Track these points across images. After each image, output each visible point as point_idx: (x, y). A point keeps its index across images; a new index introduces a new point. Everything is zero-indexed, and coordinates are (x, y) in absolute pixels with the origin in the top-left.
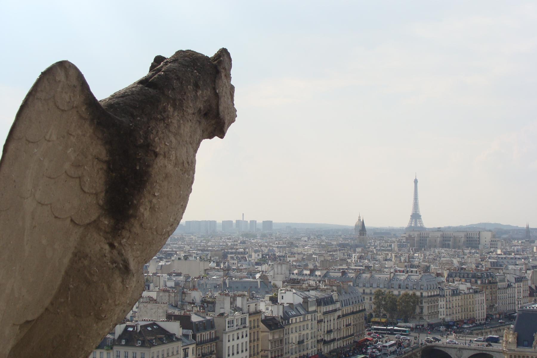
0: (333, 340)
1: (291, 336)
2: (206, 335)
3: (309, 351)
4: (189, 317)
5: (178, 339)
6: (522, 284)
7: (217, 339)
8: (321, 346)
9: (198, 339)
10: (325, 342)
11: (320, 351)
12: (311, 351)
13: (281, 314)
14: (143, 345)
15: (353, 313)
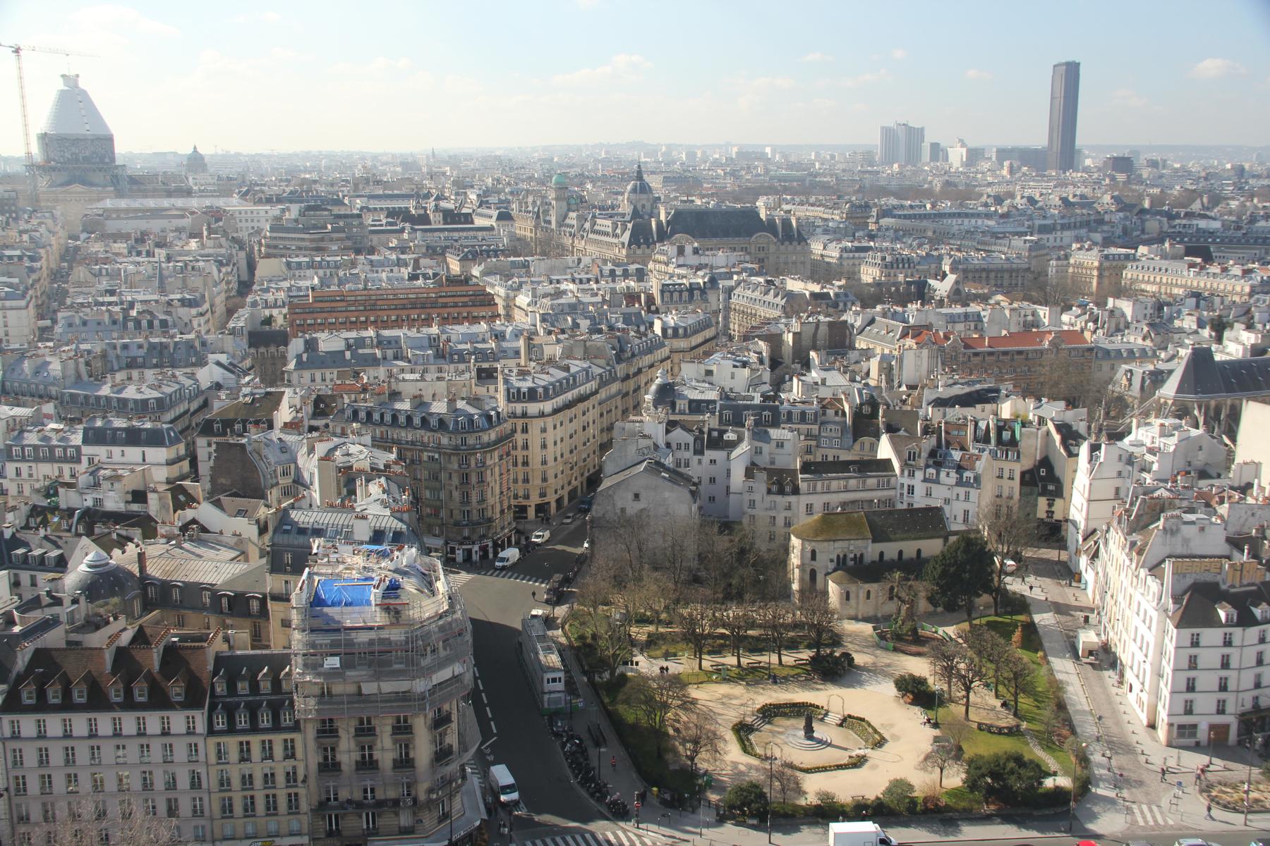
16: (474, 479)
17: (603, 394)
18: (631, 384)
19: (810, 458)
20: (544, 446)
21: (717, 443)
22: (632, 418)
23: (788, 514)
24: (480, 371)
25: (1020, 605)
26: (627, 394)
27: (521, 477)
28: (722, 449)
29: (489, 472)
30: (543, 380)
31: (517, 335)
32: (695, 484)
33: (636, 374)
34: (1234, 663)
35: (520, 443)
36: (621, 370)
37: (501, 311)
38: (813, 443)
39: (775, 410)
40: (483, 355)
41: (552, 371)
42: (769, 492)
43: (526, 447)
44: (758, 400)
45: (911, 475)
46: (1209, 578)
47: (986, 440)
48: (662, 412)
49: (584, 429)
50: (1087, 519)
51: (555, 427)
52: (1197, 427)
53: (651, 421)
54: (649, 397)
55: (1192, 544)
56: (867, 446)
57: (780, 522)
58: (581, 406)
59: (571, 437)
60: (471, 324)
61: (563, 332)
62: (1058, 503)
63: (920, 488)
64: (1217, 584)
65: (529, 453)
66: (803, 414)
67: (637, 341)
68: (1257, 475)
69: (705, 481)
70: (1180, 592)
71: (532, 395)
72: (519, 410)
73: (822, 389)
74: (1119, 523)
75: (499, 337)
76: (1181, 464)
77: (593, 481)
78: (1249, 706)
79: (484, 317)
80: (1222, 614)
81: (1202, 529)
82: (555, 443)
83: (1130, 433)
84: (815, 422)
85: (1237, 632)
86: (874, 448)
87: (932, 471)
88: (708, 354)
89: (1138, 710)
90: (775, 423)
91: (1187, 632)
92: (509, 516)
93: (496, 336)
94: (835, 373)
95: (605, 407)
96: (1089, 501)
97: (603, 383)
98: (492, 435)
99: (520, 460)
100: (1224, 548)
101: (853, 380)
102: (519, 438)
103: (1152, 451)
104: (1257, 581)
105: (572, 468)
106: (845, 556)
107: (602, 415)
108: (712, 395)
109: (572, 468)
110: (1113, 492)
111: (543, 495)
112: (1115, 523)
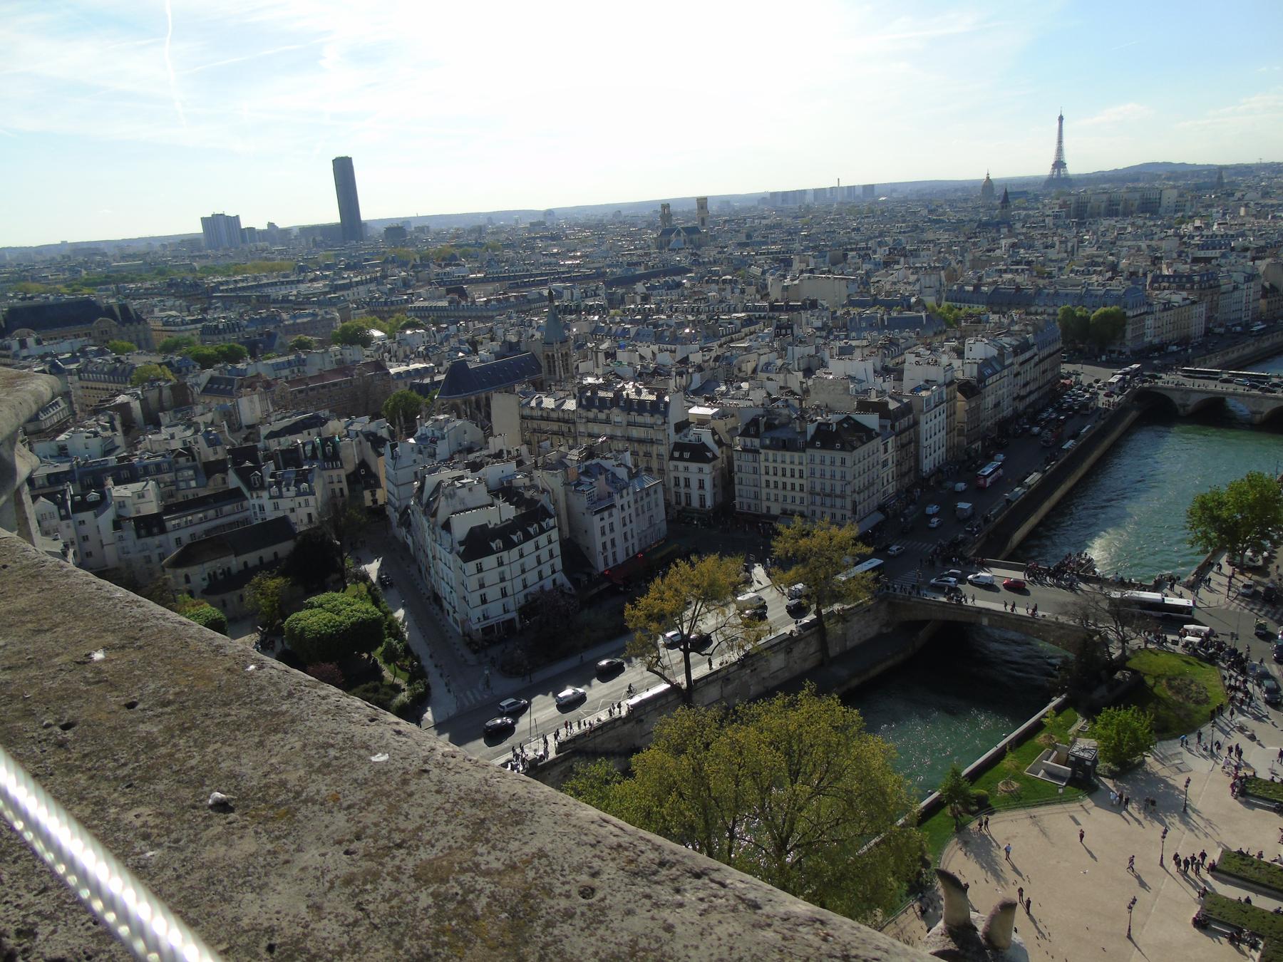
0: (1031, 393)
1: (988, 399)
2: (904, 422)
3: (1005, 414)
4: (886, 404)
5: (878, 435)
6: (1252, 284)
7: (916, 423)
8: (1017, 403)
9: (897, 429)
10: (1021, 398)
11: (1015, 410)
12: (1008, 412)
13: (975, 373)
14: (843, 449)
15: (1050, 355)
78: (523, 602)
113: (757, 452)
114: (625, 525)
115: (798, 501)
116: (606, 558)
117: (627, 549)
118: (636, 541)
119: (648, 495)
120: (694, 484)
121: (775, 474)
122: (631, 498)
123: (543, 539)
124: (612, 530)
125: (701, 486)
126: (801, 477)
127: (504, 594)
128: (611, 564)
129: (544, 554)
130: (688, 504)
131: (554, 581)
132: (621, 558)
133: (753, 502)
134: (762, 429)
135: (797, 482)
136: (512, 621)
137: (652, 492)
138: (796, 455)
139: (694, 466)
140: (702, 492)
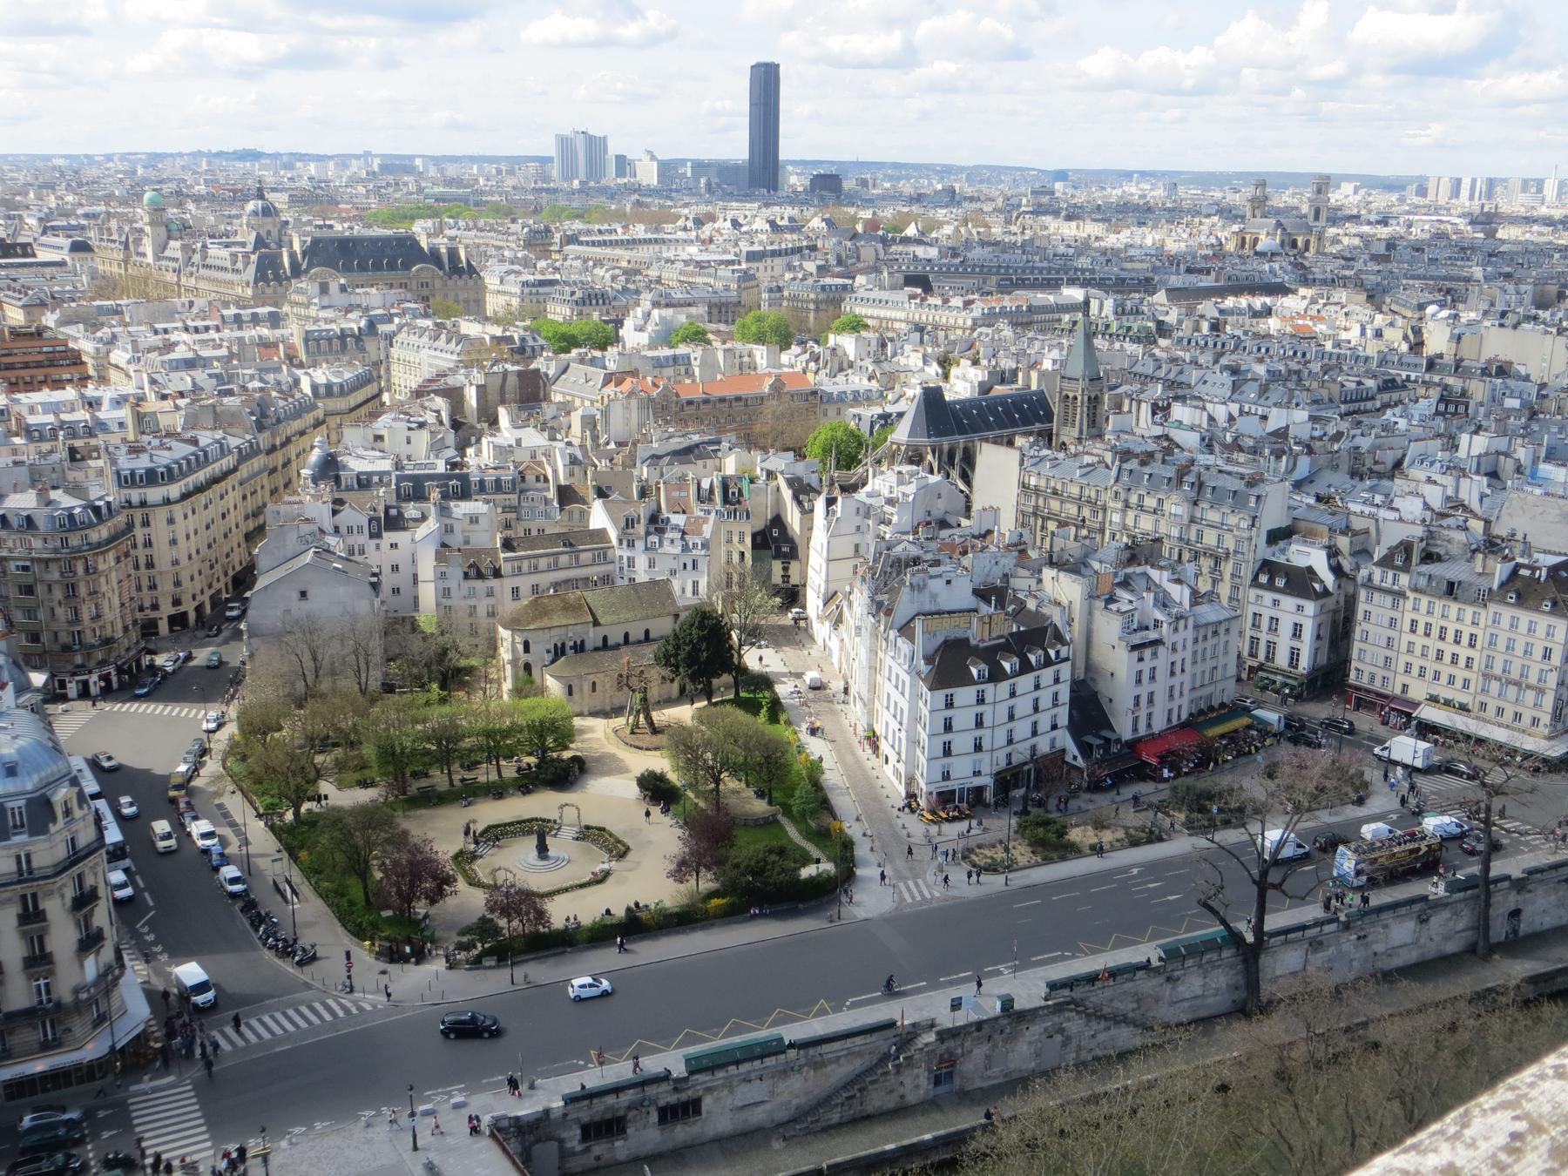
16: (83, 590)
17: (244, 471)
18: (279, 458)
19: (508, 533)
20: (174, 542)
21: (394, 522)
22: (287, 498)
23: (491, 601)
24: (73, 452)
25: (764, 682)
26: (273, 471)
27: (145, 583)
28: (405, 529)
29: (103, 580)
30: (163, 458)
31: (118, 402)
32: (374, 575)
33: (283, 445)
34: (987, 721)
35: (140, 540)
36: (264, 439)
37: (91, 372)
38: (514, 516)
39: (464, 478)
40: (72, 430)
41: (174, 444)
42: (466, 576)
43: (148, 544)
44: (441, 468)
45: (631, 545)
46: (960, 635)
47: (710, 499)
48: (325, 488)
49: (224, 516)
50: (827, 581)
51: (186, 517)
52: (931, 472)
53: (312, 502)
54: (305, 472)
55: (939, 600)
56: (576, 515)
57: (482, 611)
58: (218, 488)
59: (208, 527)
60: (53, 389)
61: (182, 395)
62: (794, 567)
63: (641, 562)
64: (967, 640)
65: (154, 551)
66: (498, 481)
67: (282, 403)
68: (996, 522)
69: (386, 570)
70: (931, 652)
71: (151, 477)
72: (135, 499)
73: (517, 451)
74: (864, 580)
75: (93, 404)
76: (921, 516)
77: (243, 579)
78: (1003, 764)
79: (70, 381)
80: (974, 671)
81: (948, 582)
82: (188, 537)
83: (864, 484)
84: (513, 491)
85: (989, 687)
86: (585, 515)
87: (655, 539)
88: (374, 415)
89: (896, 782)
90: (464, 494)
91: (941, 694)
92: (134, 635)
93: (90, 404)
94: (530, 430)
95: (248, 489)
96: (829, 560)
97: (243, 457)
98: (103, 532)
99: (142, 561)
100: (969, 601)
101: (553, 439)
102: (139, 533)
103: (891, 502)
104: (1006, 633)
105: (212, 567)
106: (563, 645)
107: (244, 498)
108: (386, 465)
109: (212, 567)
110: (852, 548)
111: (177, 602)
112: (858, 583)
113: (1401, 594)
114: (1173, 673)
115: (1459, 683)
116: (1136, 720)
117: (1170, 711)
118: (1185, 701)
119: (1215, 633)
120: (1285, 629)
121: (1427, 635)
122: (1189, 634)
123: (1047, 675)
124: (1153, 678)
125: (1297, 631)
126: (1472, 645)
127: (978, 748)
128: (1142, 731)
129: (1045, 698)
130: (1270, 656)
131: (1053, 741)
132: (1159, 725)
133: (1380, 673)
134: (1415, 559)
135: (1464, 652)
136: (979, 790)
137: (1222, 630)
138: (1469, 611)
139: (1289, 602)
140: (1295, 644)
